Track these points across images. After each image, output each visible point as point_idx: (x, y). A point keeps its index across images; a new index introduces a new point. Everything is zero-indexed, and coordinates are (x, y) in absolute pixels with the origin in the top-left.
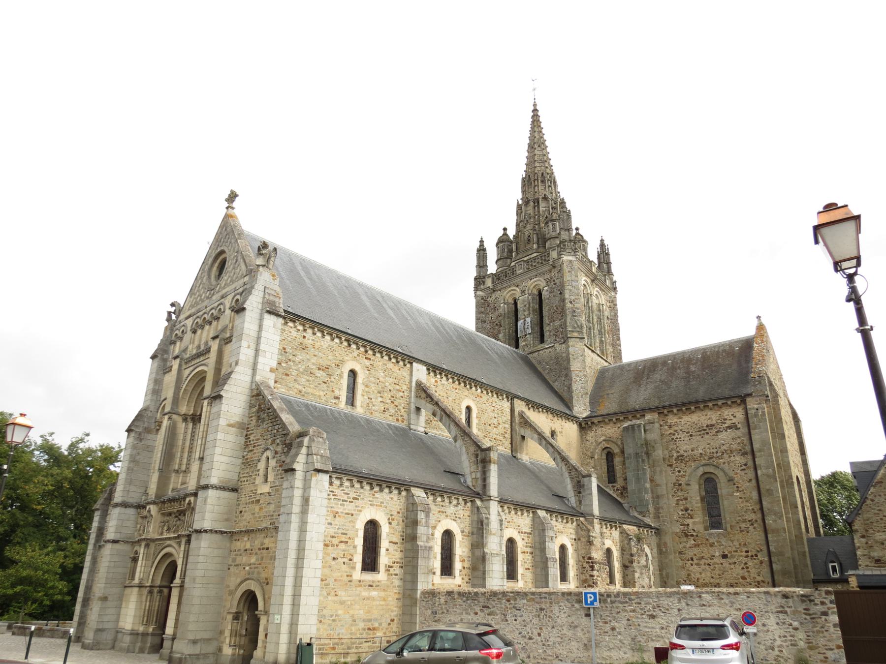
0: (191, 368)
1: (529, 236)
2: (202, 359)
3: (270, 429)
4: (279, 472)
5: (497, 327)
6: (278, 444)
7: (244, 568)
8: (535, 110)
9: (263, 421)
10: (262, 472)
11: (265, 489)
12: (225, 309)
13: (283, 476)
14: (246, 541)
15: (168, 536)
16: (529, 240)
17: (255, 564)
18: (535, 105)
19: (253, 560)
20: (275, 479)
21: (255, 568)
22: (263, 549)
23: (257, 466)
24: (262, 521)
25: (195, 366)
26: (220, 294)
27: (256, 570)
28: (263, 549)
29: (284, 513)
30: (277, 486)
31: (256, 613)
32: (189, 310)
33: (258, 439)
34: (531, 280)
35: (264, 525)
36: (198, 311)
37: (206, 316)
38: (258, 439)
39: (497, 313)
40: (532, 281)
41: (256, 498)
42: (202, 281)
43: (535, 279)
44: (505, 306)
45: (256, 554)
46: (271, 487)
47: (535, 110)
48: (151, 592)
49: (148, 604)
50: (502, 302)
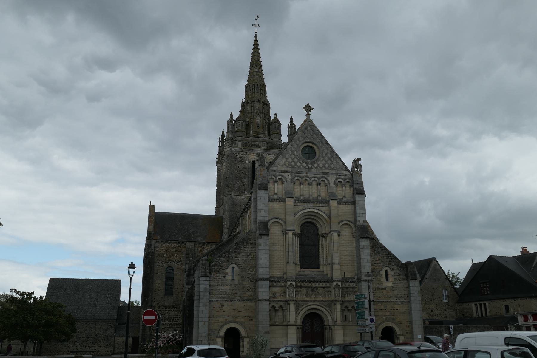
0: (301, 208)
1: (258, 124)
2: (312, 205)
3: (385, 257)
4: (398, 278)
5: (242, 174)
6: (393, 266)
7: (382, 317)
8: (256, 41)
9: (379, 253)
10: (384, 276)
11: (390, 284)
12: (329, 184)
13: (400, 280)
14: (380, 306)
15: (309, 299)
16: (258, 126)
17: (389, 316)
18: (256, 37)
19: (388, 314)
20: (395, 281)
21: (389, 317)
22: (394, 309)
23: (380, 273)
24: (389, 298)
25: (308, 207)
26: (321, 171)
27: (391, 318)
28: (394, 309)
29: (413, 296)
30: (397, 284)
31: (382, 335)
32: (282, 166)
33: (377, 261)
34: (269, 155)
35: (392, 300)
36: (299, 173)
37: (307, 178)
38: (377, 261)
39: (243, 166)
40: (270, 156)
41: (382, 287)
42: (293, 153)
43: (271, 155)
44: (249, 163)
45: (389, 311)
46: (393, 284)
47: (256, 41)
48: (298, 328)
49: (298, 334)
50: (247, 160)
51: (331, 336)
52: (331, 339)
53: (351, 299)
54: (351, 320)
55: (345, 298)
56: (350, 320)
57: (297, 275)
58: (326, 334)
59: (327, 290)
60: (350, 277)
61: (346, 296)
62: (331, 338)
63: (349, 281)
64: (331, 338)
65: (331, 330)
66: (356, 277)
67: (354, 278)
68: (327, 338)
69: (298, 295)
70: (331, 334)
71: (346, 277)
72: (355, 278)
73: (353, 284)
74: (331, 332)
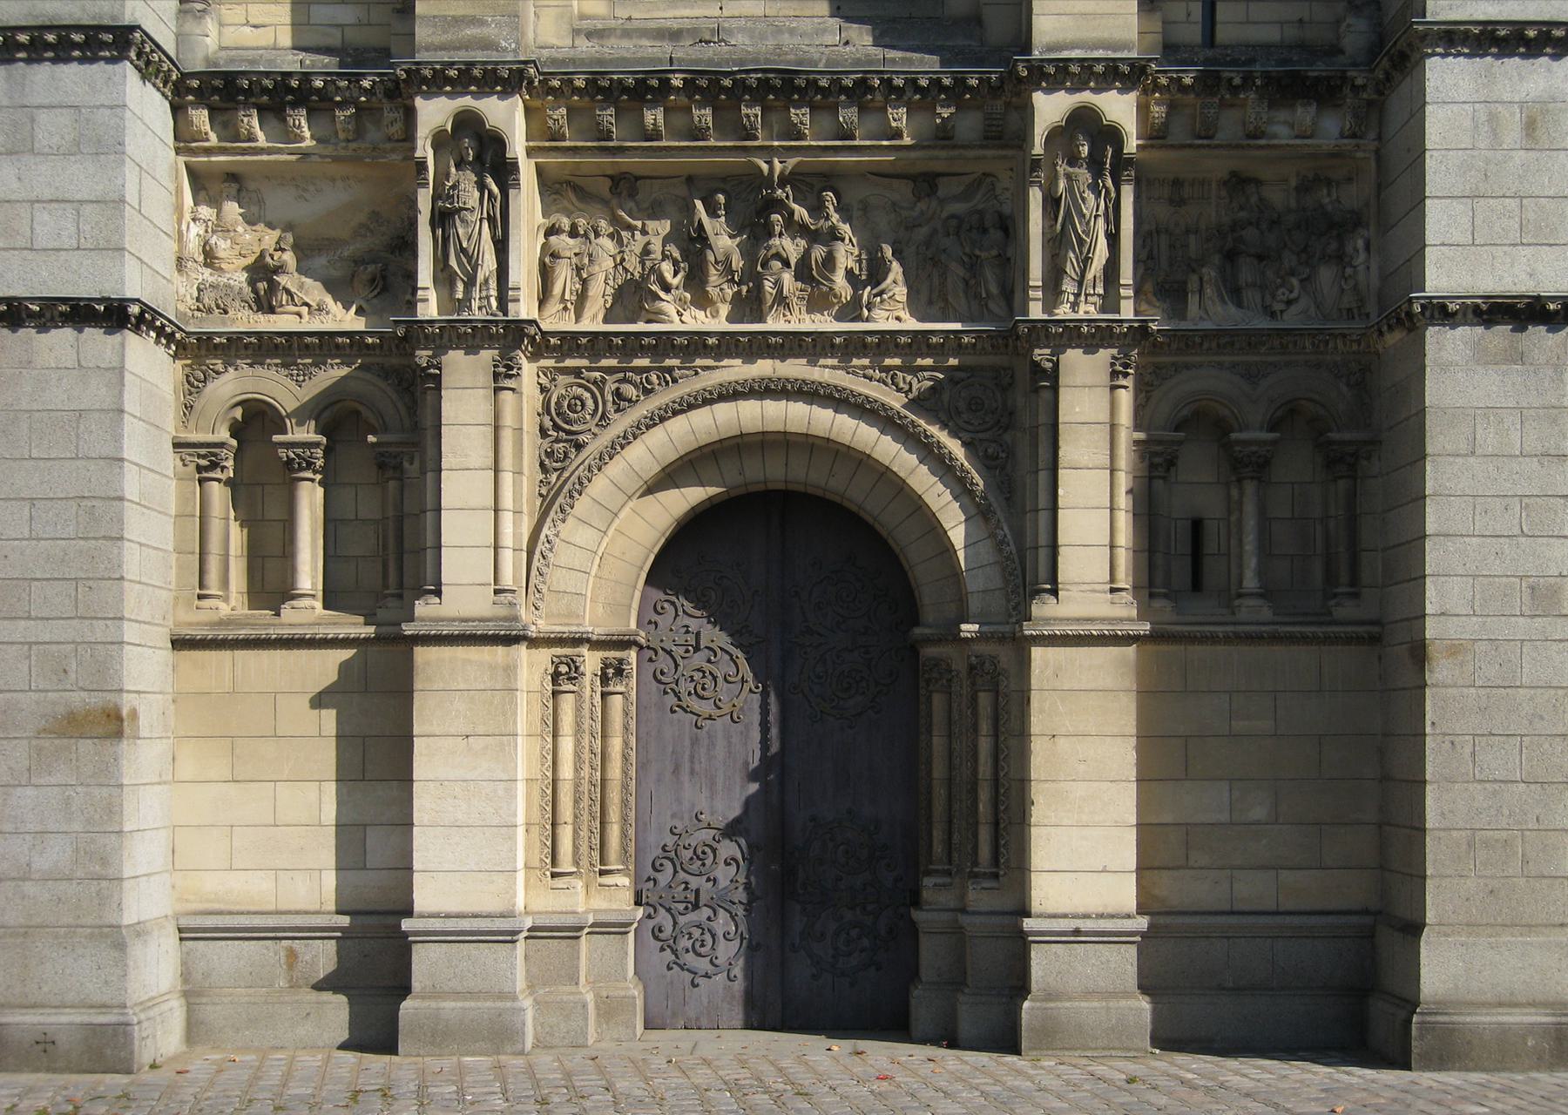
51: (985, 769)
52: (984, 807)
53: (1273, 315)
54: (1261, 573)
55: (1193, 301)
56: (1250, 582)
57: (576, 32)
58: (938, 743)
59: (958, 208)
60: (1270, 34)
61: (1210, 273)
62: (984, 795)
63: (1248, 79)
64: (984, 795)
65: (984, 699)
66: (1355, 34)
67: (1335, 50)
68: (939, 793)
69: (579, 269)
70: (985, 745)
71: (1223, 34)
72: (1342, 52)
73: (1304, 114)
74: (985, 727)
